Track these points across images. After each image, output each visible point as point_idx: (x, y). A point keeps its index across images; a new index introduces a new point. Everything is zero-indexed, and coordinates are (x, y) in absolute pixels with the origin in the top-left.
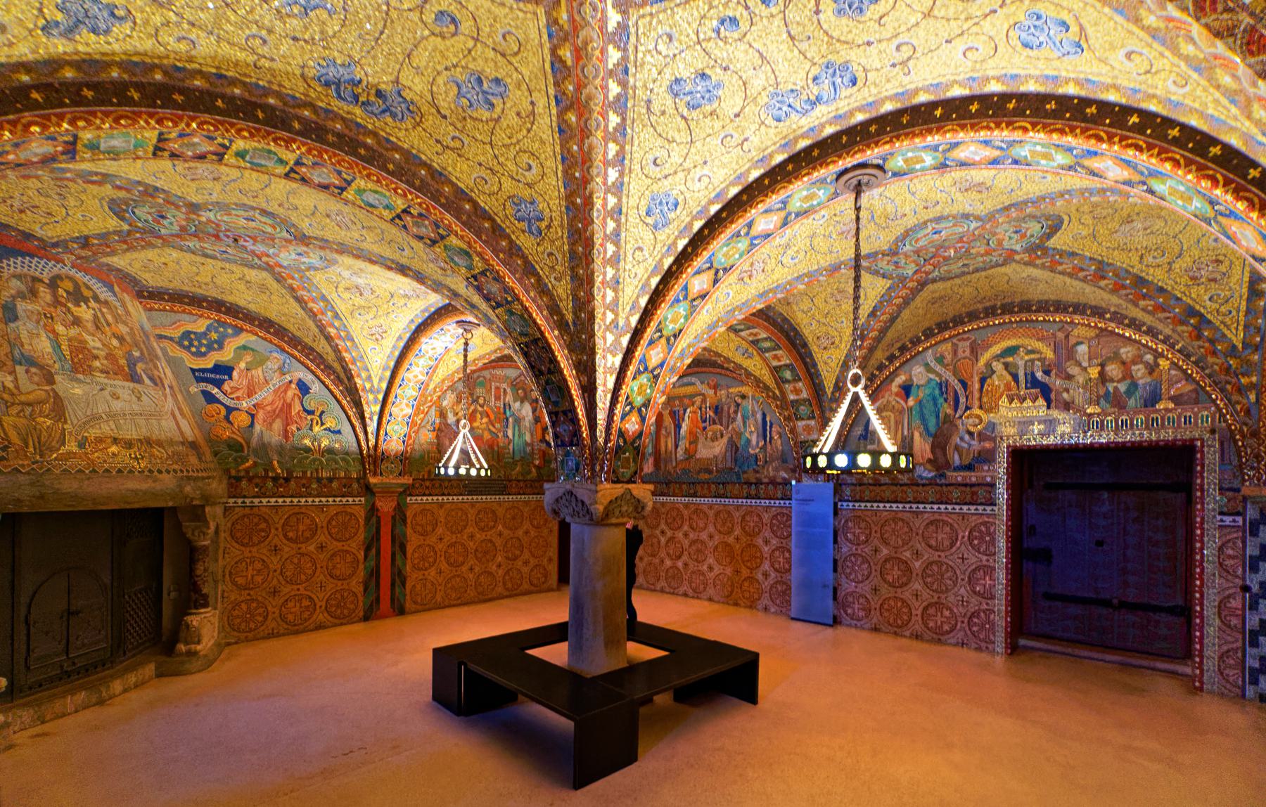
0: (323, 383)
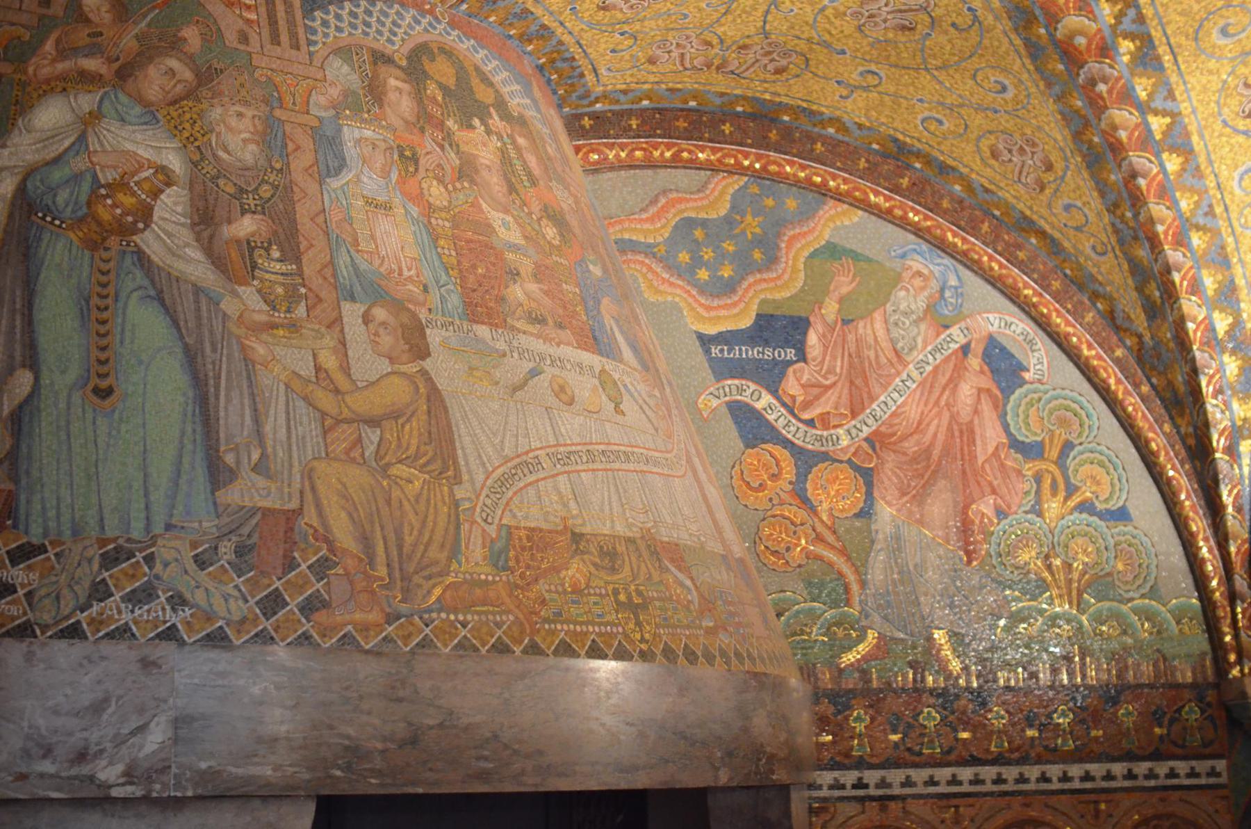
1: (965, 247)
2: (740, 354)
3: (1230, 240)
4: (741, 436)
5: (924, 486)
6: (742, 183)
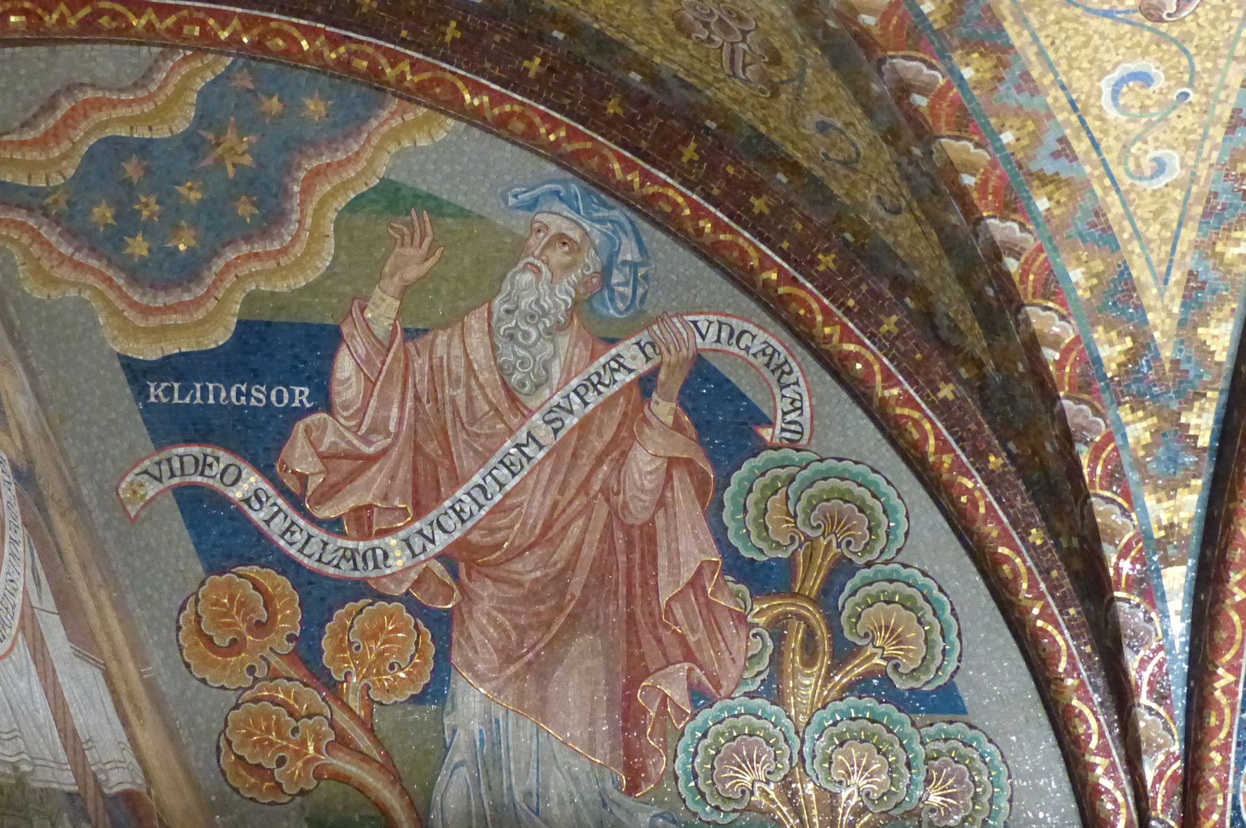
0: (836, 367)
1: (650, 189)
2: (205, 397)
3: (1113, 198)
4: (200, 551)
5: (550, 643)
6: (221, 69)
